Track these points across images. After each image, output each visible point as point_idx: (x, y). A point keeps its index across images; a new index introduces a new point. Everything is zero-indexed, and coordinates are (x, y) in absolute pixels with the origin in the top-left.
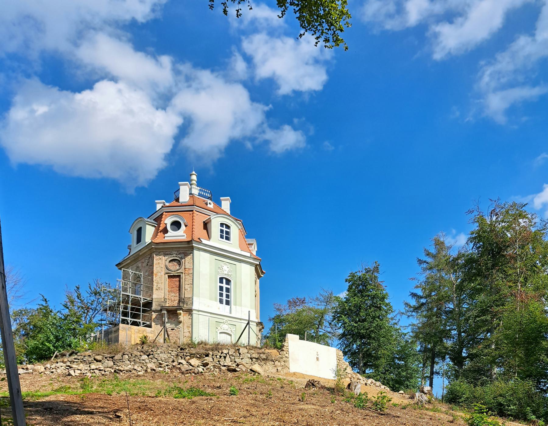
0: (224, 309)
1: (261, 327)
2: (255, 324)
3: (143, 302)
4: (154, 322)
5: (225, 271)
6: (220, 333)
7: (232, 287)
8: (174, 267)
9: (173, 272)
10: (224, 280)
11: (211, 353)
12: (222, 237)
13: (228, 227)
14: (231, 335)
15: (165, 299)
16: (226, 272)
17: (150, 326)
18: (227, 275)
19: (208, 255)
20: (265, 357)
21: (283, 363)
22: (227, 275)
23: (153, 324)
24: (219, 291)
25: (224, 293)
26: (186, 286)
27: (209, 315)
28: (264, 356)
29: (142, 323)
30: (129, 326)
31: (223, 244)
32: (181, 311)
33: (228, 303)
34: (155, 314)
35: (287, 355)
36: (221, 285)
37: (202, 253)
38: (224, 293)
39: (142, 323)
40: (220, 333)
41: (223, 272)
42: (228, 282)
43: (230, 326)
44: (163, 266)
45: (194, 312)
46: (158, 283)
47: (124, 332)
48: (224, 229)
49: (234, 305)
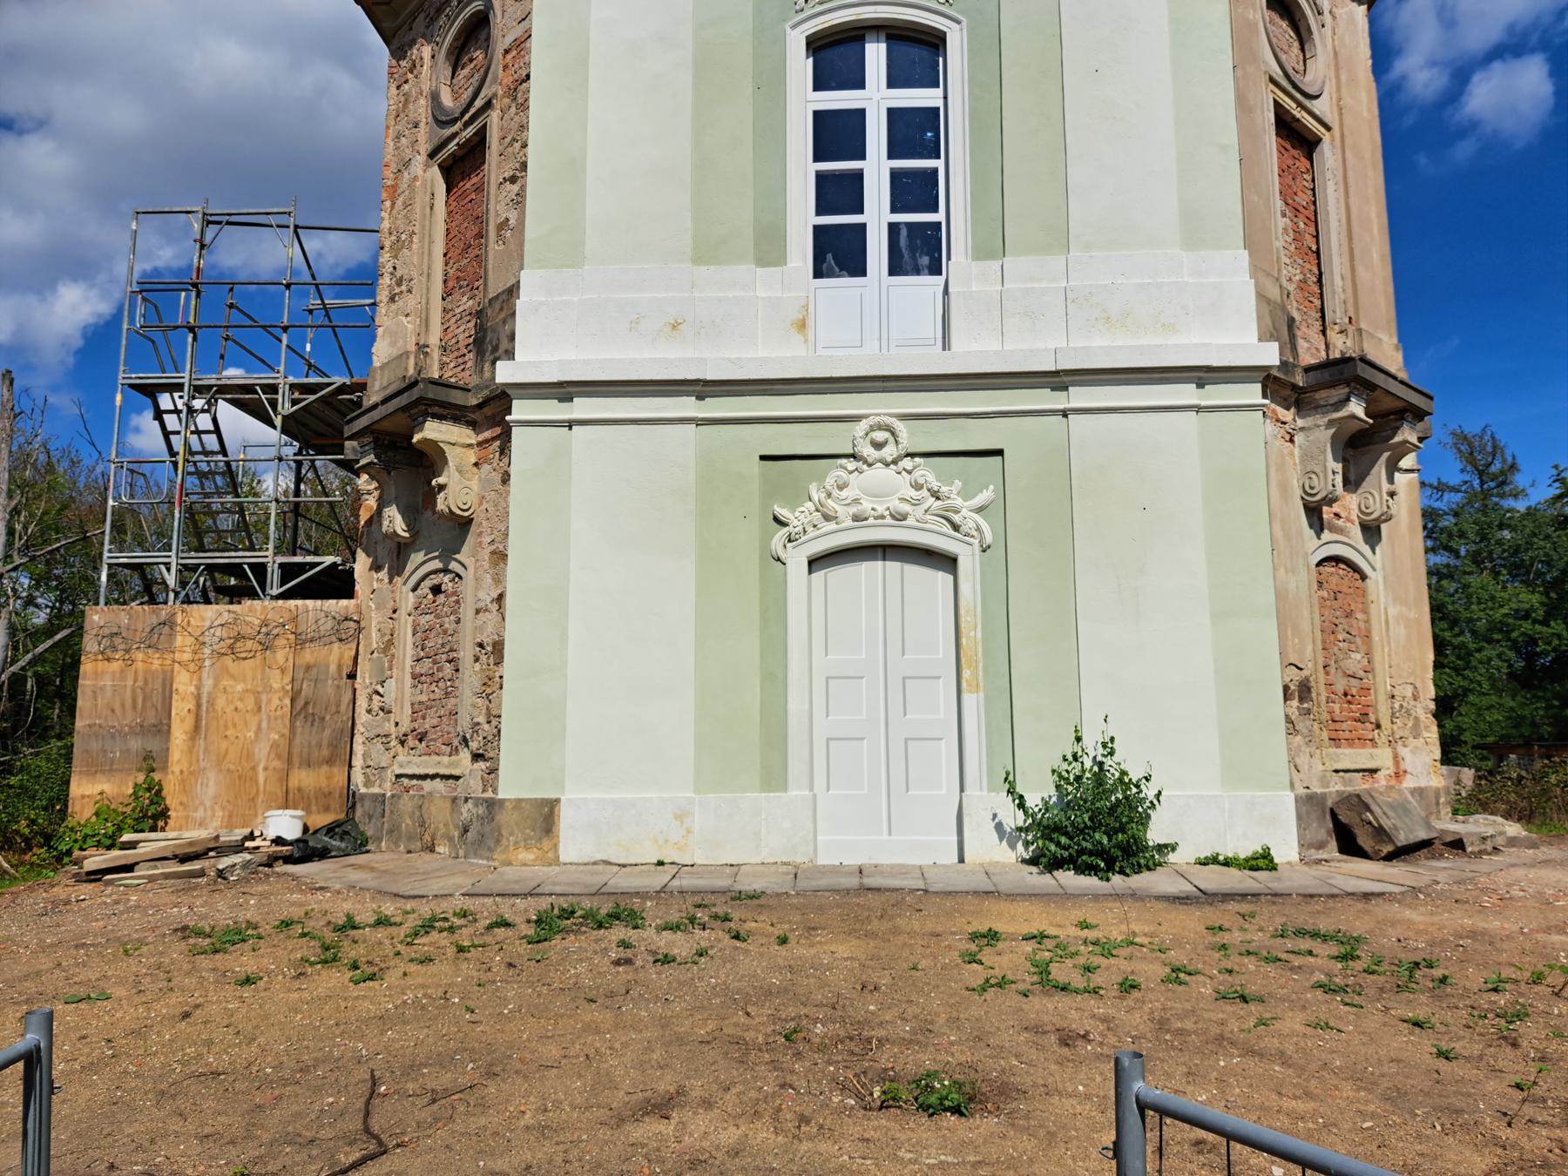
1: (1356, 408)
2: (1252, 393)
3: (285, 412)
4: (368, 555)
6: (815, 563)
9: (459, 125)
10: (876, 54)
14: (947, 562)
15: (422, 348)
17: (338, 584)
23: (361, 564)
27: (686, 406)
29: (274, 574)
32: (433, 430)
39: (274, 574)
40: (815, 563)
43: (926, 472)
45: (521, 410)
47: (116, 666)
49: (981, 252)
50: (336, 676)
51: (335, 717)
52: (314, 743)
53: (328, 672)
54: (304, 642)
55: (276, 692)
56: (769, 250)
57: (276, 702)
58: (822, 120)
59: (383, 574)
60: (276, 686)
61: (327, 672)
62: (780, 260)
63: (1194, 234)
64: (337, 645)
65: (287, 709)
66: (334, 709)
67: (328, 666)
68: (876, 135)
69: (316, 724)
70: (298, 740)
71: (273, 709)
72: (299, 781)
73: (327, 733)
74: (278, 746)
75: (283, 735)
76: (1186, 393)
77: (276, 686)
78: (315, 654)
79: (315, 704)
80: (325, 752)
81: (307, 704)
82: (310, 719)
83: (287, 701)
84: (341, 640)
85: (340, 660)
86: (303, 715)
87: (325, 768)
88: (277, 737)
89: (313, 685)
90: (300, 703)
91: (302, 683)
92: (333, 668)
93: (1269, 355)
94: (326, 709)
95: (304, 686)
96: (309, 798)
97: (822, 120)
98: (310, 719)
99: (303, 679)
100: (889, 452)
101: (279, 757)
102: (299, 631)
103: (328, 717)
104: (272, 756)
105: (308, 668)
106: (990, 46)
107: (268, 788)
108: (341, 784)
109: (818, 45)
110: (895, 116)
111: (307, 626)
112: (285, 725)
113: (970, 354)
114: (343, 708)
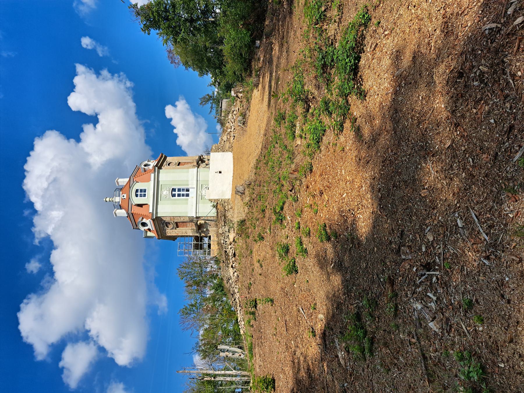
0: (192, 193)
1: (200, 162)
2: (199, 169)
7: (177, 187)
8: (171, 226)
10: (173, 193)
11: (224, 250)
12: (145, 195)
13: (137, 191)
15: (192, 229)
16: (168, 192)
19: (159, 206)
20: (223, 217)
21: (226, 204)
24: (181, 197)
25: (181, 193)
26: (182, 220)
27: (198, 205)
28: (223, 218)
30: (211, 250)
31: (150, 193)
32: (198, 223)
33: (188, 190)
35: (220, 200)
36: (177, 195)
37: (159, 211)
38: (181, 193)
42: (174, 190)
43: (203, 189)
44: (171, 231)
45: (197, 216)
46: (183, 233)
48: (139, 193)
49: (188, 186)
56: (188, 199)
58: (178, 196)
62: (188, 199)
63: (188, 172)
68: (179, 193)
76: (198, 173)
93: (196, 168)
97: (178, 196)
106: (174, 185)
109: (173, 197)
110: (178, 191)
113: (195, 186)
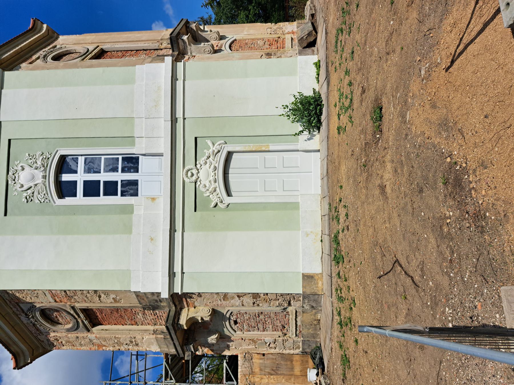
1: (185, 38)
2: (180, 65)
3: (175, 382)
4: (224, 351)
5: (33, 178)
6: (229, 194)
9: (79, 320)
10: (66, 177)
14: (230, 155)
15: (155, 332)
16: (39, 174)
17: (233, 361)
18: (45, 170)
22: (45, 170)
23: (227, 353)
24: (103, 200)
26: (108, 302)
27: (178, 235)
32: (183, 321)
34: (201, 350)
38: (103, 177)
40: (229, 194)
41: (39, 186)
43: (201, 160)
45: (177, 290)
49: (133, 144)
50: (264, 360)
51: (277, 360)
52: (286, 367)
53: (263, 363)
54: (252, 372)
55: (269, 381)
56: (129, 210)
57: (272, 381)
58: (86, 194)
59: (231, 344)
60: (267, 381)
61: (262, 363)
62: (131, 206)
63: (131, 81)
64: (253, 360)
65: (275, 377)
66: (275, 360)
67: (260, 363)
68: (92, 177)
69: (279, 366)
70: (285, 372)
71: (274, 382)
72: (298, 371)
73: (282, 362)
74: (287, 379)
75: (283, 378)
77: (267, 381)
78: (256, 368)
79: (273, 367)
80: (289, 363)
81: (273, 370)
82: (278, 368)
83: (272, 377)
84: (252, 359)
85: (258, 359)
86: (277, 371)
87: (294, 363)
88: (284, 380)
89: (266, 368)
90: (273, 372)
91: (266, 372)
92: (261, 361)
93: (169, 60)
94: (274, 363)
95: (267, 371)
96: (304, 368)
97: (86, 194)
98: (278, 368)
99: (265, 372)
100: (195, 171)
101: (290, 379)
102: (249, 374)
103: (277, 362)
104: (290, 381)
105: (261, 370)
106: (66, 140)
107: (301, 382)
108: (299, 357)
109: (61, 195)
111: (247, 371)
112: (280, 377)
113: (164, 147)
114: (274, 357)
